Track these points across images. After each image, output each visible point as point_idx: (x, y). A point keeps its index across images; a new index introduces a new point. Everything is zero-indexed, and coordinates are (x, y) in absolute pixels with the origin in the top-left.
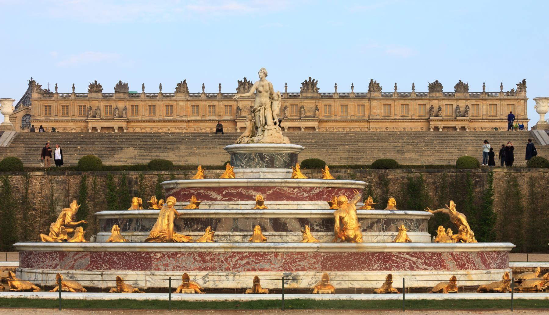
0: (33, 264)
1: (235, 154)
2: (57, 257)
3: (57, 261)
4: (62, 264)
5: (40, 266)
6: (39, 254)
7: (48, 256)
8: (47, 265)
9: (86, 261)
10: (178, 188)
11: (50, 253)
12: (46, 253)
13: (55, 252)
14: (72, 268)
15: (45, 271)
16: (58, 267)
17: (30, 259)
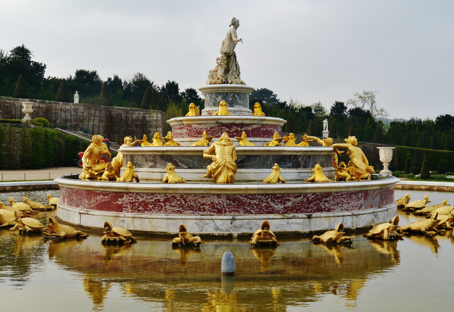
0: (332, 207)
1: (238, 94)
2: (362, 196)
3: (362, 201)
4: (366, 204)
5: (343, 208)
6: (342, 195)
7: (354, 197)
8: (352, 206)
9: (378, 199)
10: (258, 124)
11: (356, 193)
12: (351, 193)
13: (360, 192)
14: (372, 207)
15: (355, 212)
16: (363, 207)
17: (327, 201)
